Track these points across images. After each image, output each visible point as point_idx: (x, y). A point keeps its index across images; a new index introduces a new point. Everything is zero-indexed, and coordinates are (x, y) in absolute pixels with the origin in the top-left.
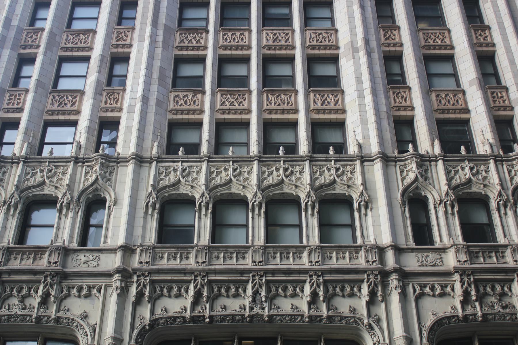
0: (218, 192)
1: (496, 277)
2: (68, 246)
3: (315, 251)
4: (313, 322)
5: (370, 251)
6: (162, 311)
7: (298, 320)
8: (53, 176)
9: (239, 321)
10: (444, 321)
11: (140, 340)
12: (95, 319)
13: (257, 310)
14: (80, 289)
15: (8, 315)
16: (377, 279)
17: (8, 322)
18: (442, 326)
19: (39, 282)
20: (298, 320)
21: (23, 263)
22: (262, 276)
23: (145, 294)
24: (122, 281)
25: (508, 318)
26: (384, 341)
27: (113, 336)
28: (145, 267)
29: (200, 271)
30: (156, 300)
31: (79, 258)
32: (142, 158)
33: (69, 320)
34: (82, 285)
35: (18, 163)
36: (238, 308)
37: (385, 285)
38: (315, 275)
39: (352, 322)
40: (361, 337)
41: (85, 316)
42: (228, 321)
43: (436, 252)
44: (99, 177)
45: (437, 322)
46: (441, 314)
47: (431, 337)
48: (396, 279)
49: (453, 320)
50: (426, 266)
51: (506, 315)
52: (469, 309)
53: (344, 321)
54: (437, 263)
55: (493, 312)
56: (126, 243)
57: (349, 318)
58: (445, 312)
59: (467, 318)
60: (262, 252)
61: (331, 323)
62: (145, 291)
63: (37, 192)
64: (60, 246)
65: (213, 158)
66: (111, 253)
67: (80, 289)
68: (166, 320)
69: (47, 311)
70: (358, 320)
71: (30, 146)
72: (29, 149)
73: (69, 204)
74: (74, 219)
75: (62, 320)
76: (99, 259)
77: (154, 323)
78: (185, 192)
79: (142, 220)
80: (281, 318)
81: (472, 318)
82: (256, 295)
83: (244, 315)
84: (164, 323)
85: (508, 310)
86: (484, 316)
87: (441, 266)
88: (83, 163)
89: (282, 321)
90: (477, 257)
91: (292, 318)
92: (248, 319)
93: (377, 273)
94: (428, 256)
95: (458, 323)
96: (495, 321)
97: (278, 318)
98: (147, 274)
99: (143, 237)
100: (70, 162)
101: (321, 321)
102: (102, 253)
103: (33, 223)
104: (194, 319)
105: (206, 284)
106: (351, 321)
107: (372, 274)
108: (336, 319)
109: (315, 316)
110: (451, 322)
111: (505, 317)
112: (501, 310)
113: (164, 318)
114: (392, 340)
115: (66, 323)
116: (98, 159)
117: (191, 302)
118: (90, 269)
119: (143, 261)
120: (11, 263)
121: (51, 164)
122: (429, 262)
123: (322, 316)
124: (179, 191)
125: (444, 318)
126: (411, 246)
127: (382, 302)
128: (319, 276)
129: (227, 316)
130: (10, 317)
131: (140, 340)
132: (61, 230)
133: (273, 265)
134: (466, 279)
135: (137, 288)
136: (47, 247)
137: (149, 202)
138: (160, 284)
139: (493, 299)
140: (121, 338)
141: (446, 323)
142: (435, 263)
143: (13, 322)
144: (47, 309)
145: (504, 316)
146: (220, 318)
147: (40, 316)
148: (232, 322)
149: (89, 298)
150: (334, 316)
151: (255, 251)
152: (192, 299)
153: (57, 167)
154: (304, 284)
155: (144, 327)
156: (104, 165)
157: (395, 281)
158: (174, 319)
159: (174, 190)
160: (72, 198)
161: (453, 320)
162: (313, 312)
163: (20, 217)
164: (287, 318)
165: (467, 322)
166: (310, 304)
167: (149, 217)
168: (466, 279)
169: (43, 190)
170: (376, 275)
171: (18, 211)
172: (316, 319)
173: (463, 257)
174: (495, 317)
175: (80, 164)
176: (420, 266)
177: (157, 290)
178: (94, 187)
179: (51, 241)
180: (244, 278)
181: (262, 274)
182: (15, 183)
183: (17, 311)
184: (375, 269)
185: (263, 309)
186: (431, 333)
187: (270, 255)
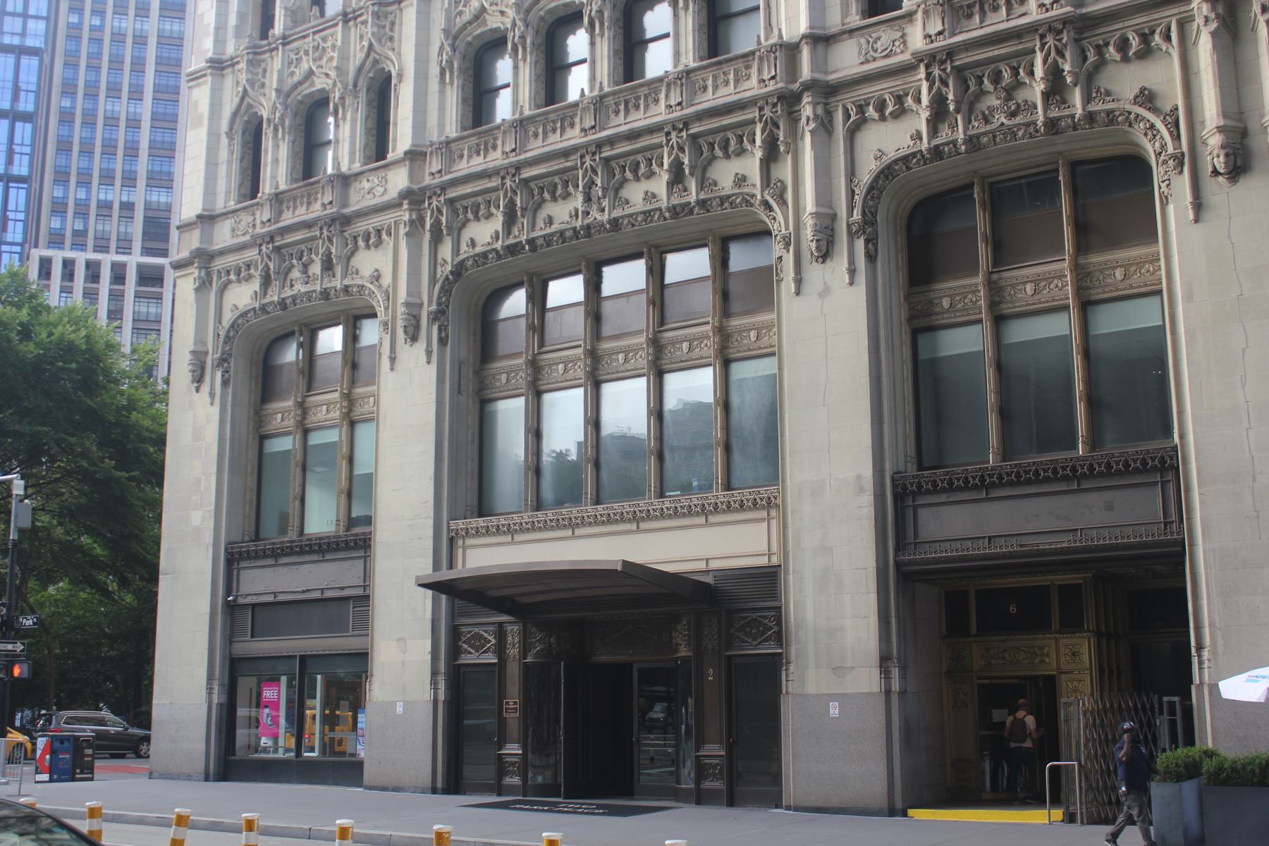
0: (541, 9)
1: (996, 53)
2: (843, 25)
3: (675, 83)
4: (680, 216)
5: (765, 59)
6: (468, 246)
7: (656, 217)
8: (320, 58)
9: (571, 239)
10: (896, 167)
11: (444, 299)
12: (387, 280)
13: (595, 214)
14: (881, 107)
15: (291, 296)
16: (777, 111)
17: (295, 305)
18: (894, 178)
19: (753, 122)
20: (656, 217)
21: (297, 213)
22: (594, 154)
23: (778, 139)
24: (411, 210)
25: (1020, 133)
26: (787, 228)
27: (814, 211)
28: (941, 43)
29: (506, 168)
30: (460, 230)
31: (361, 186)
32: (221, 62)
33: (358, 286)
34: (367, 229)
35: (277, 49)
36: (567, 218)
37: (793, 118)
38: (674, 130)
39: (741, 203)
40: (1138, 145)
41: (377, 277)
42: (557, 241)
43: (895, 26)
44: (373, 40)
45: (882, 172)
46: (892, 155)
47: (871, 203)
48: (808, 103)
49: (914, 161)
50: (875, 59)
51: (1015, 129)
52: (945, 134)
53: (726, 204)
54: (894, 48)
55: (988, 128)
56: (811, 28)
57: (734, 197)
58: (899, 149)
59: (940, 151)
60: (595, 110)
61: (708, 211)
62: (778, 135)
63: (306, 90)
64: (333, 175)
65: (290, 36)
66: (400, 167)
67: (881, 107)
68: (475, 260)
69: (333, 279)
70: (749, 198)
71: (289, 13)
72: (288, 19)
73: (342, 98)
74: (354, 121)
75: (709, 203)
76: (386, 180)
77: (459, 270)
78: (495, 26)
79: (437, 95)
80: (631, 219)
81: (950, 149)
82: (590, 188)
83: (576, 227)
84: (473, 266)
85: (1018, 118)
86: (969, 140)
87: (902, 52)
88: (355, 18)
89: (633, 225)
90: (970, 16)
91: (647, 217)
92: (582, 232)
93: (775, 100)
94: (879, 38)
95: (926, 164)
96: (1016, 140)
97: (625, 222)
98: (439, 192)
99: (441, 125)
100: (336, 25)
101: (691, 212)
102: (389, 170)
103: (649, 35)
104: (513, 250)
105: (518, 188)
106: (738, 201)
107: (767, 104)
108: (714, 204)
109: (681, 205)
110: (911, 165)
111: (1015, 134)
112: (1005, 121)
113: (471, 256)
114: (801, 224)
115: (357, 292)
116: (368, 7)
117: (1042, 91)
118: (378, 200)
119: (587, 128)
120: (284, 216)
121: (317, 37)
122: (880, 51)
123: (690, 203)
124: (487, 25)
125: (896, 162)
126: (851, 25)
127: (1076, 85)
128: (681, 131)
129: (552, 234)
130: (294, 298)
131: (444, 299)
132: (341, 144)
133: (614, 127)
134: (936, 72)
135: (1045, 61)
136: (753, 53)
137: (442, 61)
138: (706, 138)
139: (993, 101)
140: (419, 302)
141: (901, 169)
142: (892, 50)
143: (300, 304)
144: (334, 277)
145: (1011, 133)
146: (545, 240)
147: (325, 289)
148: (563, 242)
149: (380, 247)
150: (710, 199)
151: (583, 110)
152: (928, 114)
153: (324, 39)
154: (1034, 58)
155: (447, 278)
156: (380, 14)
157: (807, 106)
158: (485, 255)
159: (480, 27)
160: (345, 89)
161: (914, 161)
162: (676, 201)
163: (696, 10)
164: (639, 219)
165: (942, 159)
166: (671, 185)
167: (448, 87)
168: (936, 72)
169: (313, 84)
170: (775, 105)
171: (456, 74)
172: (684, 208)
173: (936, 26)
174: (994, 137)
175: (351, 23)
176: (862, 63)
177: (1089, 54)
178: (371, 59)
179: (579, 92)
180: (569, 164)
181: (594, 149)
182: (275, 86)
183: (300, 288)
184: (770, 94)
185: (603, 210)
186: (869, 197)
187: (610, 109)
